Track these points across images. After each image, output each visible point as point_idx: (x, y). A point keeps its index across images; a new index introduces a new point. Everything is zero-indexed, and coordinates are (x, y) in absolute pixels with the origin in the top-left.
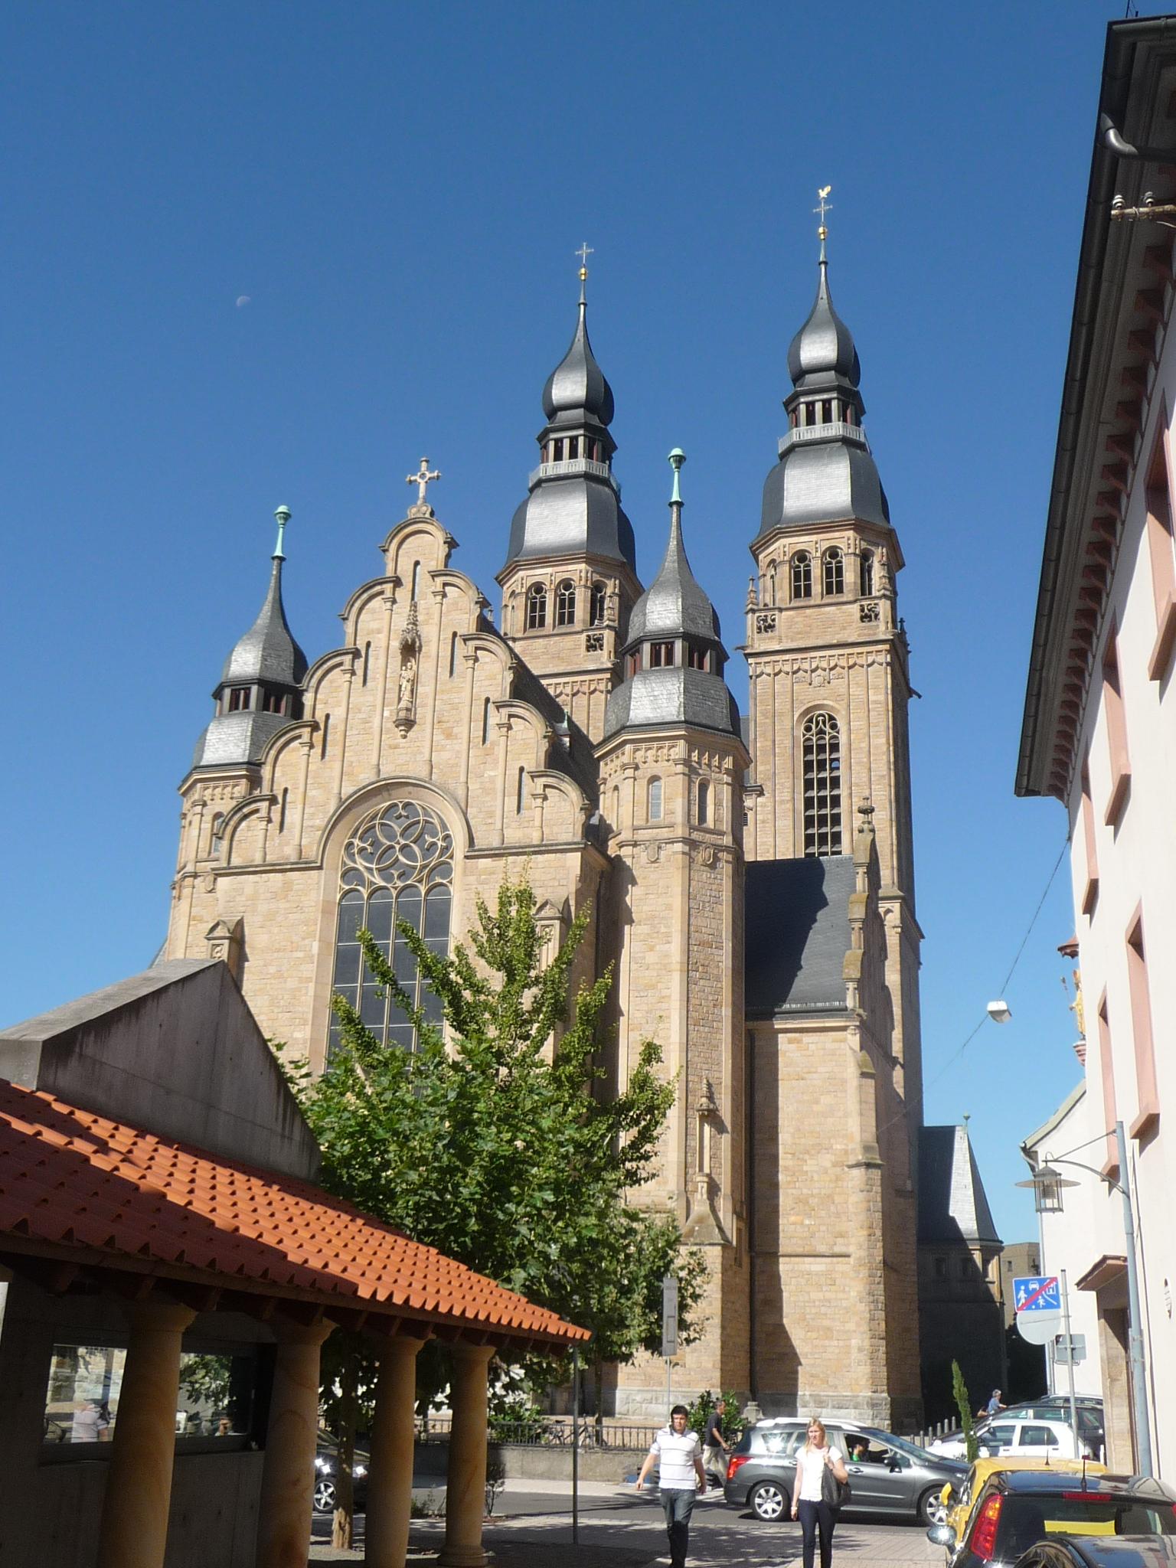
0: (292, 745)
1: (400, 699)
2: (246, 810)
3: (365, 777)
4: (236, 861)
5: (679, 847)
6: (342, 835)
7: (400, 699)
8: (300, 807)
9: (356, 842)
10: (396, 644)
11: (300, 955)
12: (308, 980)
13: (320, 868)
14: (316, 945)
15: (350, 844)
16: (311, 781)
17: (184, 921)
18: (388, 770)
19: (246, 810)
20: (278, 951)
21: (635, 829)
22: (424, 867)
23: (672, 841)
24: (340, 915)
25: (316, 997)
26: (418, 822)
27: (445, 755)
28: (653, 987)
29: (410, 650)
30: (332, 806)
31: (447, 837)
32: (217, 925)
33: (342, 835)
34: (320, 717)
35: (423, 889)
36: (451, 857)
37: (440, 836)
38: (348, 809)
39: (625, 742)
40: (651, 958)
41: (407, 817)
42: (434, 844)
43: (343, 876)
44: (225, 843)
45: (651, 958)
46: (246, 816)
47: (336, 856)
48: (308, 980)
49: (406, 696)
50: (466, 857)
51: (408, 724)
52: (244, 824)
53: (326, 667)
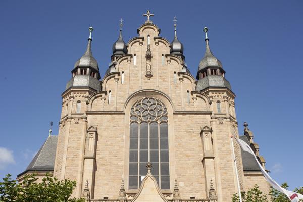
0: (111, 79)
1: (147, 69)
2: (97, 96)
3: (137, 89)
4: (93, 110)
5: (228, 120)
6: (130, 105)
7: (147, 69)
8: (115, 96)
9: (135, 108)
10: (144, 55)
11: (119, 139)
12: (122, 147)
13: (124, 114)
14: (124, 137)
15: (133, 108)
16: (118, 91)
17: (68, 131)
18: (145, 88)
19: (97, 96)
20: (111, 138)
21: (215, 114)
22: (158, 116)
23: (226, 118)
24: (131, 128)
25: (125, 152)
26: (155, 104)
27: (163, 86)
28: (225, 157)
29: (149, 57)
30: (127, 97)
31: (165, 108)
32: (92, 127)
33: (130, 105)
34: (120, 71)
35: (159, 122)
36: (167, 114)
37: (163, 108)
38: (133, 97)
39: (209, 91)
40: (224, 149)
41: (151, 102)
42: (161, 110)
43: (131, 117)
44: (90, 105)
45: (224, 149)
46: (96, 98)
47: (128, 111)
48: (122, 147)
49: (150, 68)
50: (174, 114)
51: (149, 76)
52: (96, 100)
53: (123, 58)
